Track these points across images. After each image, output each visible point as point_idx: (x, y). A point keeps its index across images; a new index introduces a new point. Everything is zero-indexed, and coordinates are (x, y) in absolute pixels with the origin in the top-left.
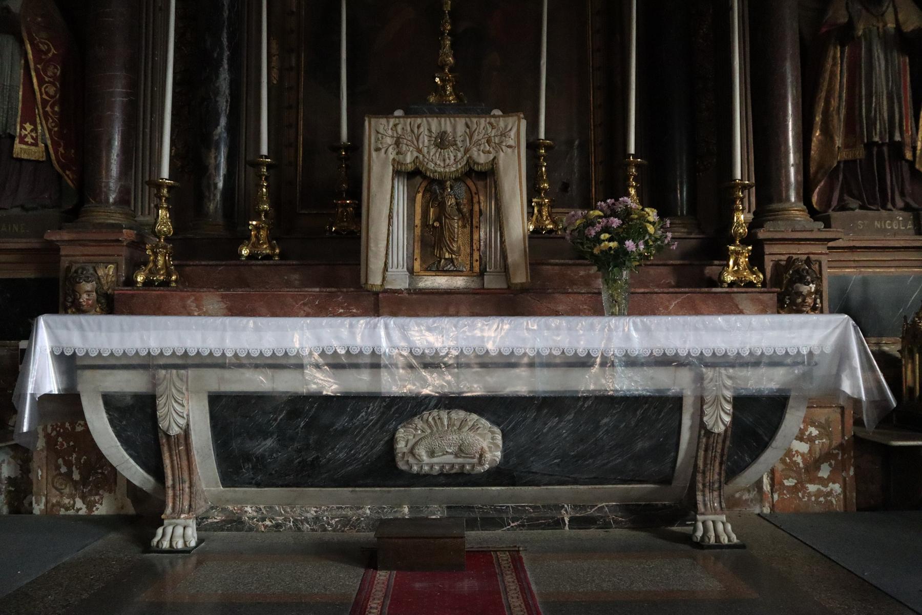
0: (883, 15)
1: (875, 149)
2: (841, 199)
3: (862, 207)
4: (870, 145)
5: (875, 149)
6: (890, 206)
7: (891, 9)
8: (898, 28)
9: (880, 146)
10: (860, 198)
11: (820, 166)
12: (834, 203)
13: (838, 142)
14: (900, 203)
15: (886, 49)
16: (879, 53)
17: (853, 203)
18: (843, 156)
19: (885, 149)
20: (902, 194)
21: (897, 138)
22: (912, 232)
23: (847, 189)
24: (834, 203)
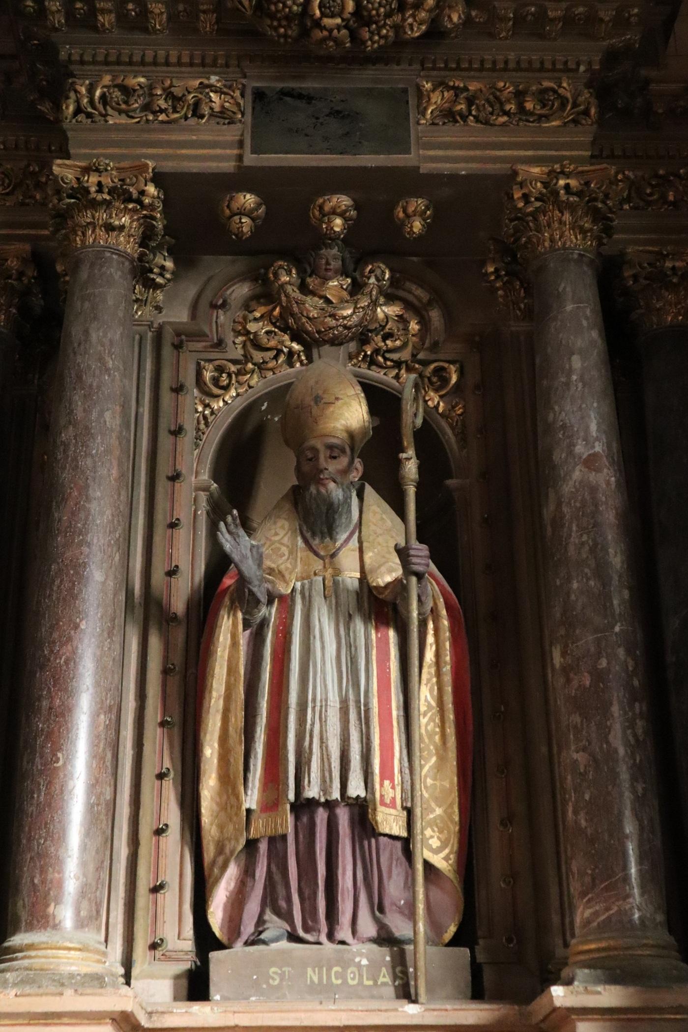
0: (333, 556)
1: (321, 815)
2: (260, 921)
3: (293, 937)
4: (304, 807)
5: (321, 815)
6: (344, 932)
7: (354, 543)
8: (363, 579)
9: (330, 805)
10: (288, 917)
11: (220, 849)
12: (248, 928)
13: (252, 799)
14: (367, 927)
15: (343, 618)
16: (325, 624)
17: (275, 926)
18: (260, 828)
19: (343, 815)
20: (379, 908)
21: (356, 789)
22: (390, 991)
23: (272, 900)
24: (248, 928)
